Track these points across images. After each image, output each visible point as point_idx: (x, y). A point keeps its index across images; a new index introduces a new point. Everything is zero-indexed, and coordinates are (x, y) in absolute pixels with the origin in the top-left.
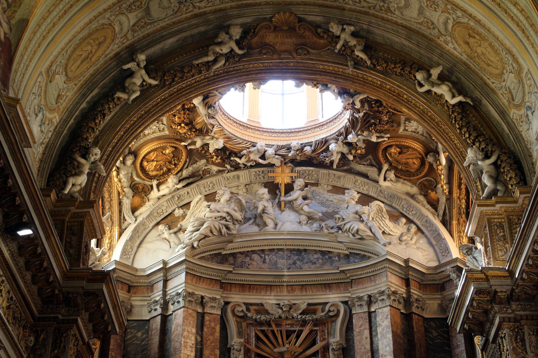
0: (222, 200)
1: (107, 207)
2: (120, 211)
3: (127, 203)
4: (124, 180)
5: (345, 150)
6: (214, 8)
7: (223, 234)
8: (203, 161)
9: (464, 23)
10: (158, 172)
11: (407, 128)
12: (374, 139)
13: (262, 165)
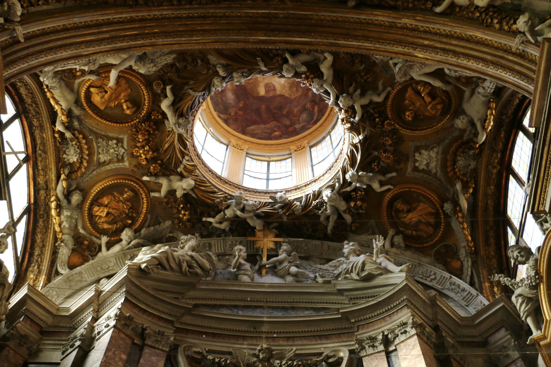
0: (187, 247)
1: (36, 253)
2: (53, 262)
3: (64, 252)
4: (65, 224)
5: (342, 206)
7: (184, 269)
8: (168, 223)
10: (110, 227)
11: (417, 164)
12: (376, 186)
13: (240, 228)
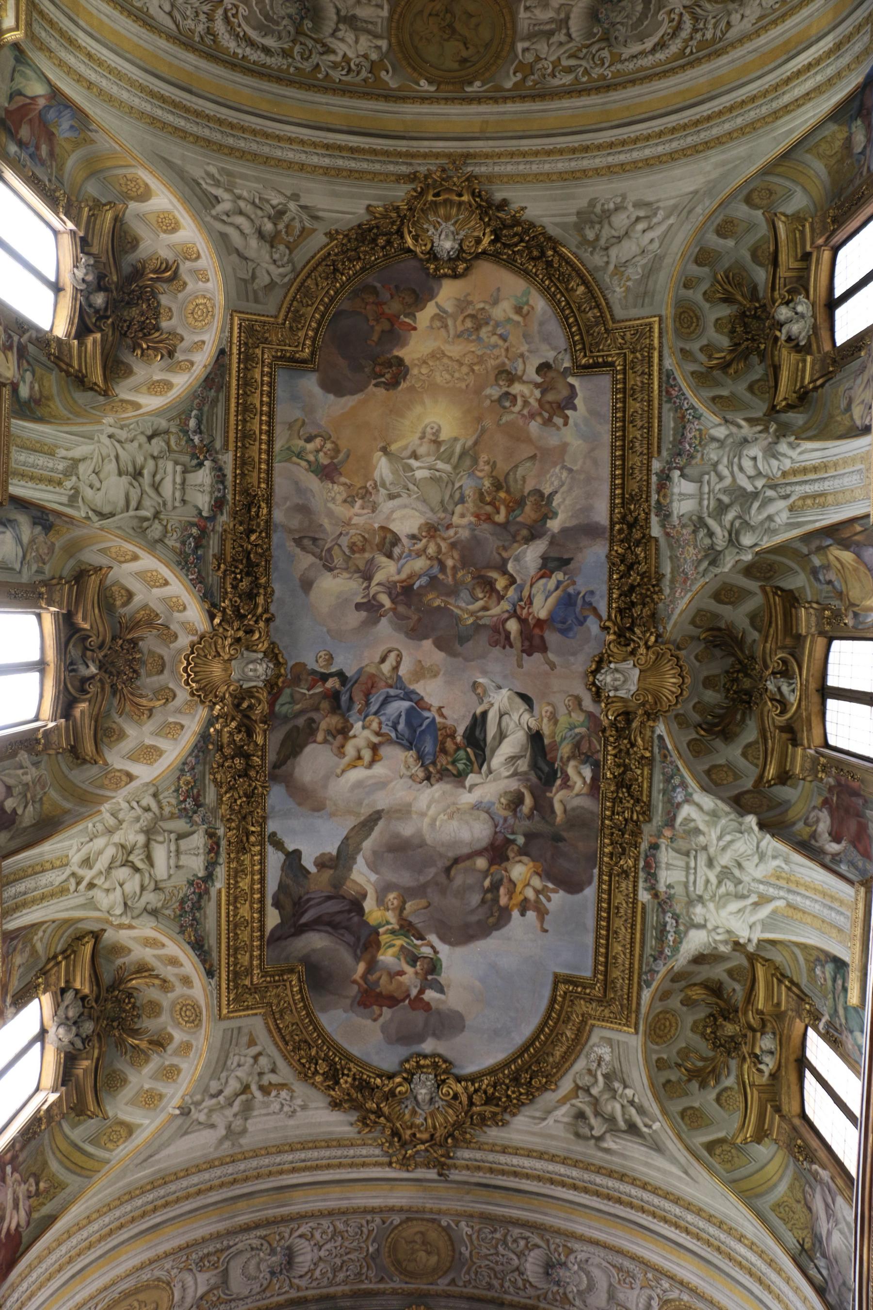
6: (318, 1291)
9: (673, 1300)
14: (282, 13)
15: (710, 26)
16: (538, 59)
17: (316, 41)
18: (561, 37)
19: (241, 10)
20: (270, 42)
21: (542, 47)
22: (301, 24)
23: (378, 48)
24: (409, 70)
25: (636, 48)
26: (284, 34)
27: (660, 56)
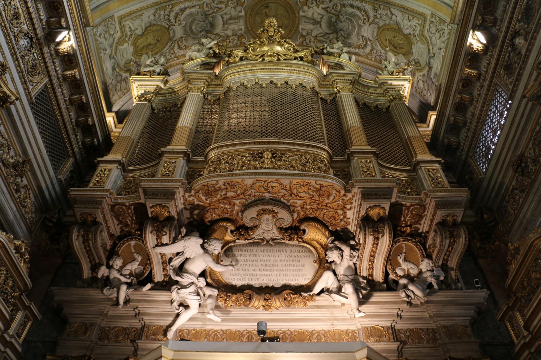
14: (344, 23)
15: (162, 16)
16: (235, 8)
17: (330, 13)
18: (226, 17)
19: (362, 22)
20: (350, 10)
21: (234, 13)
22: (337, 19)
23: (304, 12)
24: (290, 2)
25: (193, 10)
26: (344, 14)
27: (182, 6)
